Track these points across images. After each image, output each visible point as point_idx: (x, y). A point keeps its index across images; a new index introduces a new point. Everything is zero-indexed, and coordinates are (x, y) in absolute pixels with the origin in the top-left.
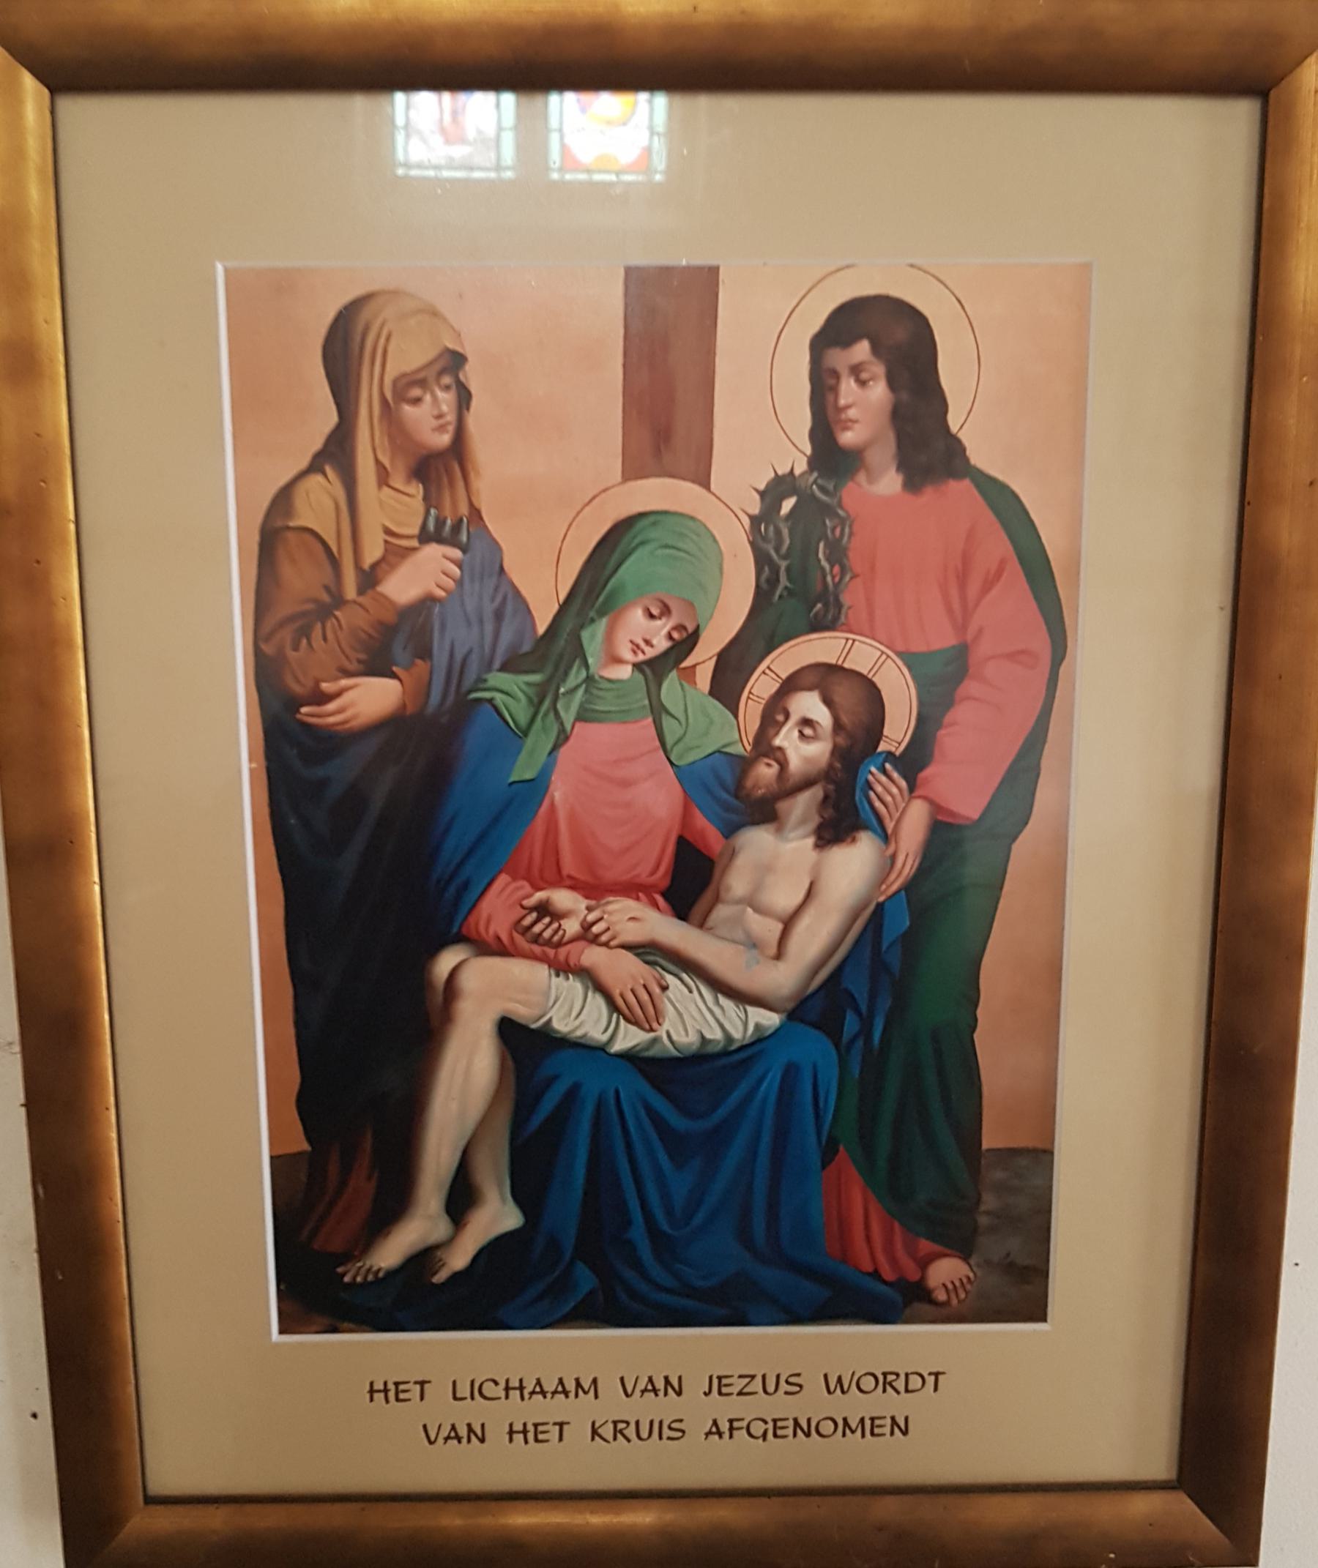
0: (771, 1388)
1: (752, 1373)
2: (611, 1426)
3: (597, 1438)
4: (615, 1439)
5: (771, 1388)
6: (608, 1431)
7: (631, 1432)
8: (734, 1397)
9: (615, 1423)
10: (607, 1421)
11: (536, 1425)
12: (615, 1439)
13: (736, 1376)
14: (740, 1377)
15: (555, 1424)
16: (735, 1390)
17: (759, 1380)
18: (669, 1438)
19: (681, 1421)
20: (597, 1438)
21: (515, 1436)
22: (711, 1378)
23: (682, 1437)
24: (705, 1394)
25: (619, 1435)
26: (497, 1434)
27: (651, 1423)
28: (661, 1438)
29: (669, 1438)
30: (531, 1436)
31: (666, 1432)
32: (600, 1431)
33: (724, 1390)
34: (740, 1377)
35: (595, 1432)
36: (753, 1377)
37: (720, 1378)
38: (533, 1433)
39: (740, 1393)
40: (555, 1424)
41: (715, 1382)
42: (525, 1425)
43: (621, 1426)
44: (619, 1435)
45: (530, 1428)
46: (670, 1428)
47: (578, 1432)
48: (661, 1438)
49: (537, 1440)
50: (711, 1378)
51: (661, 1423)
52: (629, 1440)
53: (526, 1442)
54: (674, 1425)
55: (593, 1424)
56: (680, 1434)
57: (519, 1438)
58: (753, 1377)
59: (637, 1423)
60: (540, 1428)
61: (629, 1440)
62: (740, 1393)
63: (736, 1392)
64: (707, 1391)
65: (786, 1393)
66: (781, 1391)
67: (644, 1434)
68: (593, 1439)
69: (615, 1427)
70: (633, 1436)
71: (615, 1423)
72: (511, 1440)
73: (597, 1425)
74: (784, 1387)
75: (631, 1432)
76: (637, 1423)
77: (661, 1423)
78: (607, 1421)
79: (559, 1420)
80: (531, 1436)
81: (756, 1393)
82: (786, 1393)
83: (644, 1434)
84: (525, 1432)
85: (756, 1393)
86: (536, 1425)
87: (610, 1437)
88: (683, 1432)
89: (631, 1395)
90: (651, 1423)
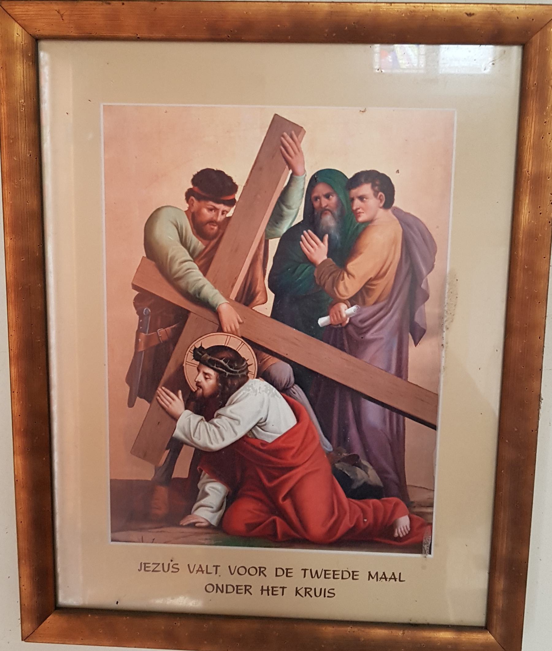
0: (166, 569)
1: (159, 562)
2: (304, 590)
3: (298, 595)
4: (306, 595)
5: (166, 569)
6: (302, 592)
7: (312, 592)
8: (151, 572)
9: (306, 589)
10: (302, 588)
11: (273, 588)
12: (306, 595)
13: (152, 563)
14: (153, 564)
15: (281, 587)
16: (151, 569)
17: (161, 565)
18: (328, 597)
19: (334, 589)
20: (298, 595)
21: (264, 592)
22: (141, 563)
23: (334, 596)
24: (139, 570)
25: (307, 594)
26: (256, 590)
27: (321, 589)
28: (325, 596)
29: (328, 597)
30: (270, 592)
31: (327, 594)
32: (299, 592)
33: (147, 569)
34: (153, 564)
35: (297, 592)
36: (159, 564)
37: (145, 564)
38: (271, 591)
39: (153, 571)
40: (281, 587)
41: (143, 566)
42: (268, 587)
43: (308, 590)
44: (247, 592)
45: (270, 589)
46: (329, 592)
47: (290, 592)
48: (325, 596)
49: (273, 594)
50: (141, 563)
51: (325, 590)
52: (311, 597)
53: (268, 595)
54: (330, 591)
55: (297, 588)
56: (333, 595)
57: (265, 593)
58: (159, 564)
59: (315, 589)
60: (275, 589)
61: (311, 597)
62: (153, 571)
63: (152, 570)
64: (140, 569)
65: (172, 572)
66: (170, 571)
67: (318, 594)
68: (296, 595)
69: (306, 590)
70: (313, 594)
71: (306, 589)
72: (262, 594)
73: (298, 589)
74: (171, 569)
75: (312, 592)
76: (315, 589)
77: (325, 590)
78: (302, 588)
79: (282, 586)
80: (270, 592)
81: (160, 571)
82: (172, 572)
83: (318, 594)
84: (268, 590)
85: (160, 571)
86: (273, 588)
87: (303, 595)
88: (334, 594)
89: (233, 574)
90: (321, 589)
